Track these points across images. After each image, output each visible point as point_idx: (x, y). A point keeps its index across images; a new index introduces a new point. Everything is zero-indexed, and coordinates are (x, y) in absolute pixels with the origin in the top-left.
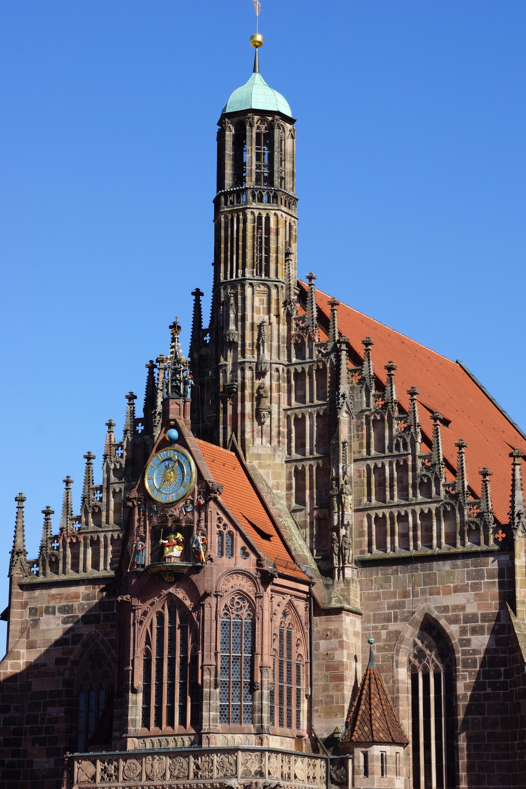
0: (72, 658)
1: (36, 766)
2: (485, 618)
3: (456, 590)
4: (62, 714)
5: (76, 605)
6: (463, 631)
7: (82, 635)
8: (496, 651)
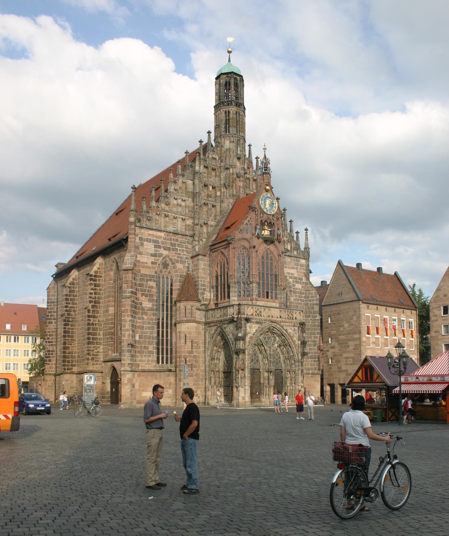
0: (159, 262)
1: (143, 305)
2: (299, 279)
3: (292, 268)
4: (155, 285)
5: (160, 241)
6: (293, 282)
7: (162, 254)
8: (302, 290)
